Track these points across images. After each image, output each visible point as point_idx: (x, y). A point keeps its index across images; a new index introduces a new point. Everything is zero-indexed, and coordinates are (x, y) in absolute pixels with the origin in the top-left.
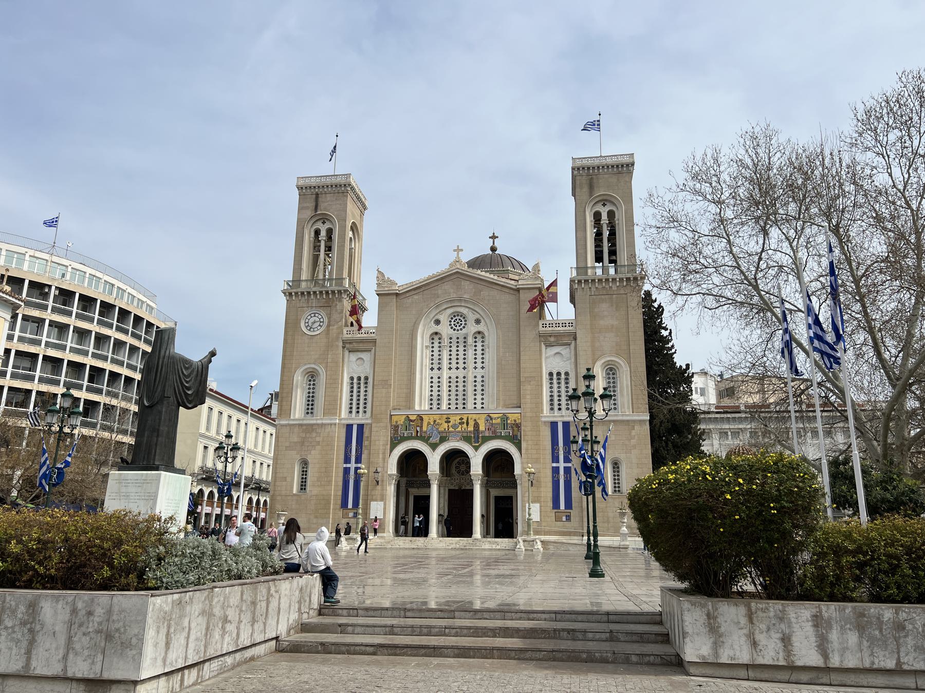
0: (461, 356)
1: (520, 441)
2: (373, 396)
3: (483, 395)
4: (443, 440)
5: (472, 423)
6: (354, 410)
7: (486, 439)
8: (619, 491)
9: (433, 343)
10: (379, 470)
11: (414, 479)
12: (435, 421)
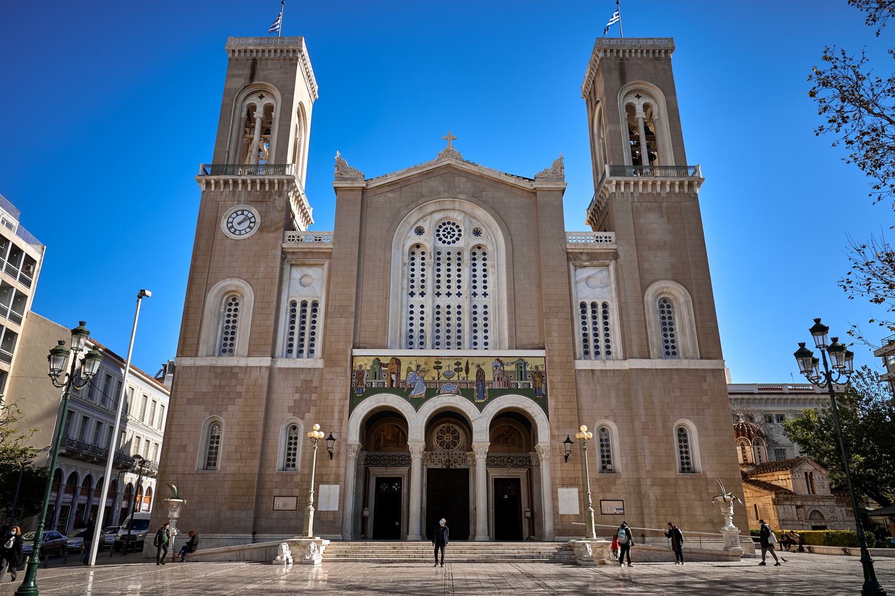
0: (454, 278)
1: (545, 397)
2: (325, 327)
3: (486, 331)
4: (431, 393)
5: (473, 371)
6: (295, 349)
7: (495, 394)
8: (689, 469)
9: (413, 259)
10: (334, 436)
11: (378, 453)
12: (418, 366)
